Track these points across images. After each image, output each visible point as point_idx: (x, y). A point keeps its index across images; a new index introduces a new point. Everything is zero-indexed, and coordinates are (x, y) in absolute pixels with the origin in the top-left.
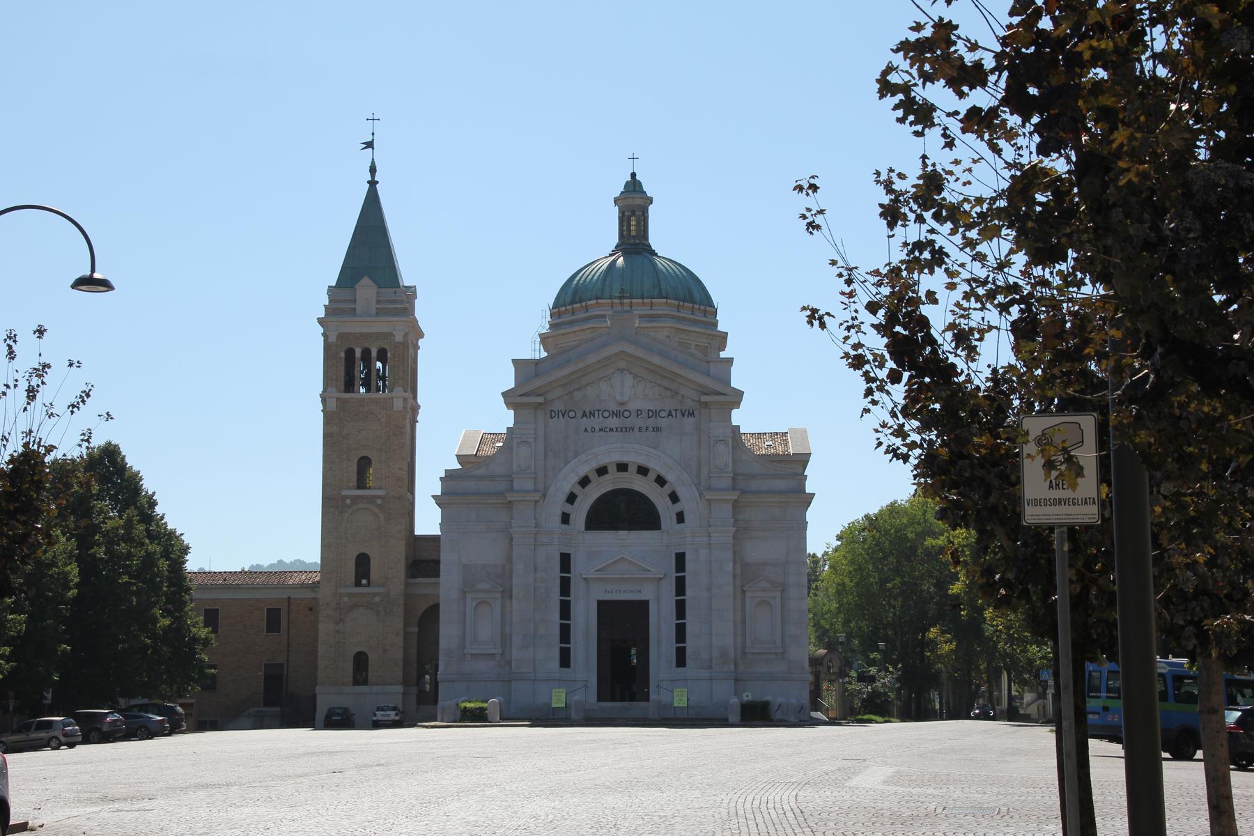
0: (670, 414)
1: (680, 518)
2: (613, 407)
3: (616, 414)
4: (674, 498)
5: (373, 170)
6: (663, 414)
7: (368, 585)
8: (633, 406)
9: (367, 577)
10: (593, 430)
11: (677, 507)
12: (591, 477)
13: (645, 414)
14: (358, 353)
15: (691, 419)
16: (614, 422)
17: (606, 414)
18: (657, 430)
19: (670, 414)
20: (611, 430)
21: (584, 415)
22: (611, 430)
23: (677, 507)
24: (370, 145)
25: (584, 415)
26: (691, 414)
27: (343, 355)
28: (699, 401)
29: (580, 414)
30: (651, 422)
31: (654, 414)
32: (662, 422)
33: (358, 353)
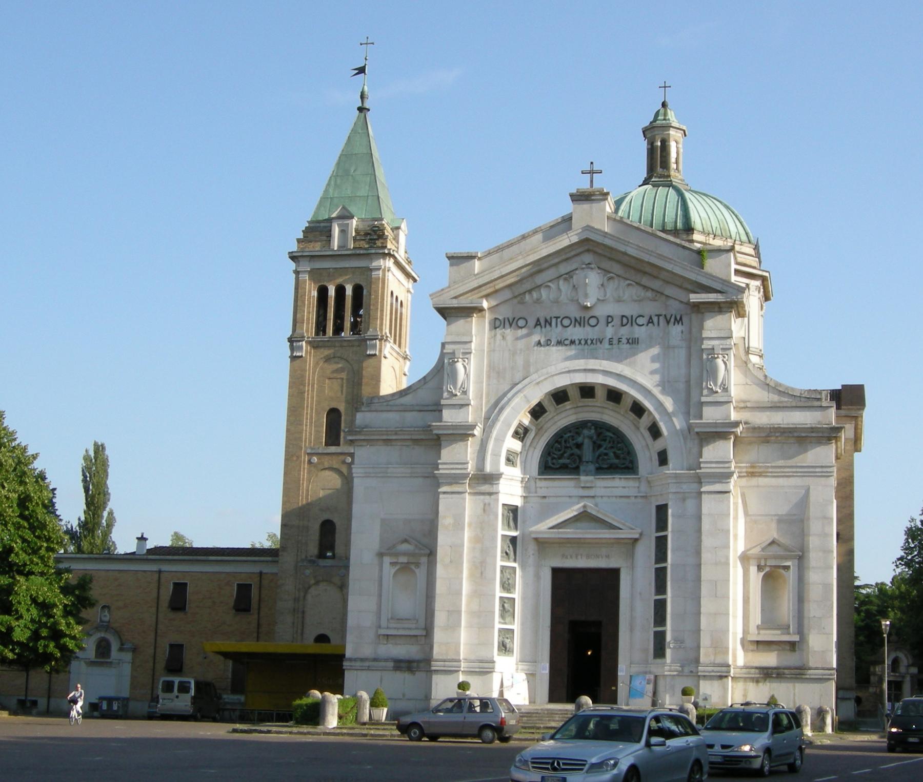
0: (650, 321)
1: (663, 458)
2: (575, 313)
3: (579, 322)
4: (655, 432)
5: (362, 96)
6: (641, 321)
7: (333, 557)
8: (602, 311)
9: (332, 548)
10: (548, 343)
11: (659, 445)
12: (546, 404)
13: (617, 321)
14: (332, 292)
15: (676, 330)
16: (576, 333)
17: (566, 322)
18: (633, 341)
19: (650, 321)
20: (572, 342)
21: (538, 323)
22: (572, 342)
23: (659, 445)
24: (362, 70)
25: (538, 323)
26: (679, 321)
27: (315, 293)
28: (688, 303)
29: (532, 322)
30: (625, 332)
31: (627, 321)
32: (640, 332)
33: (332, 292)
